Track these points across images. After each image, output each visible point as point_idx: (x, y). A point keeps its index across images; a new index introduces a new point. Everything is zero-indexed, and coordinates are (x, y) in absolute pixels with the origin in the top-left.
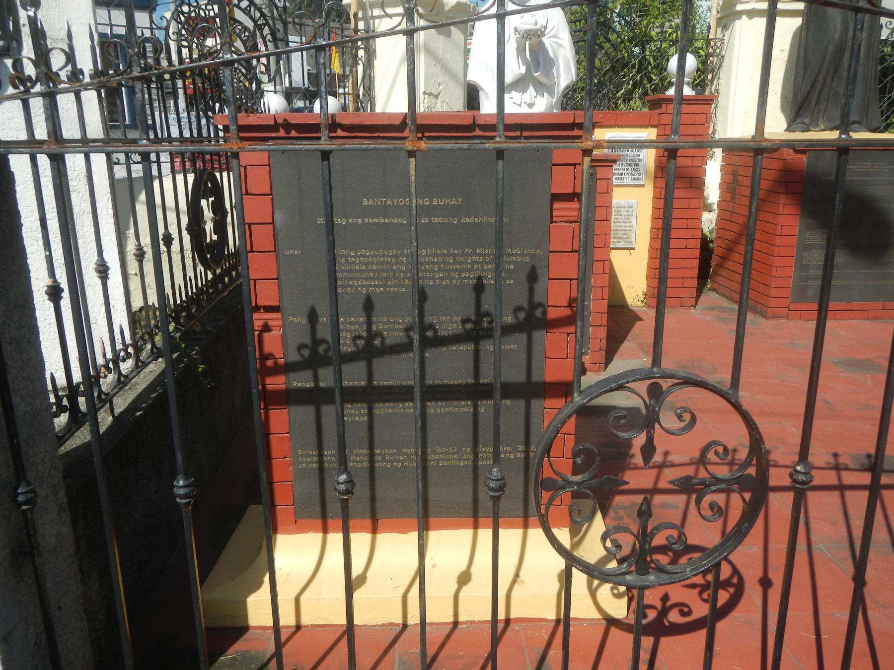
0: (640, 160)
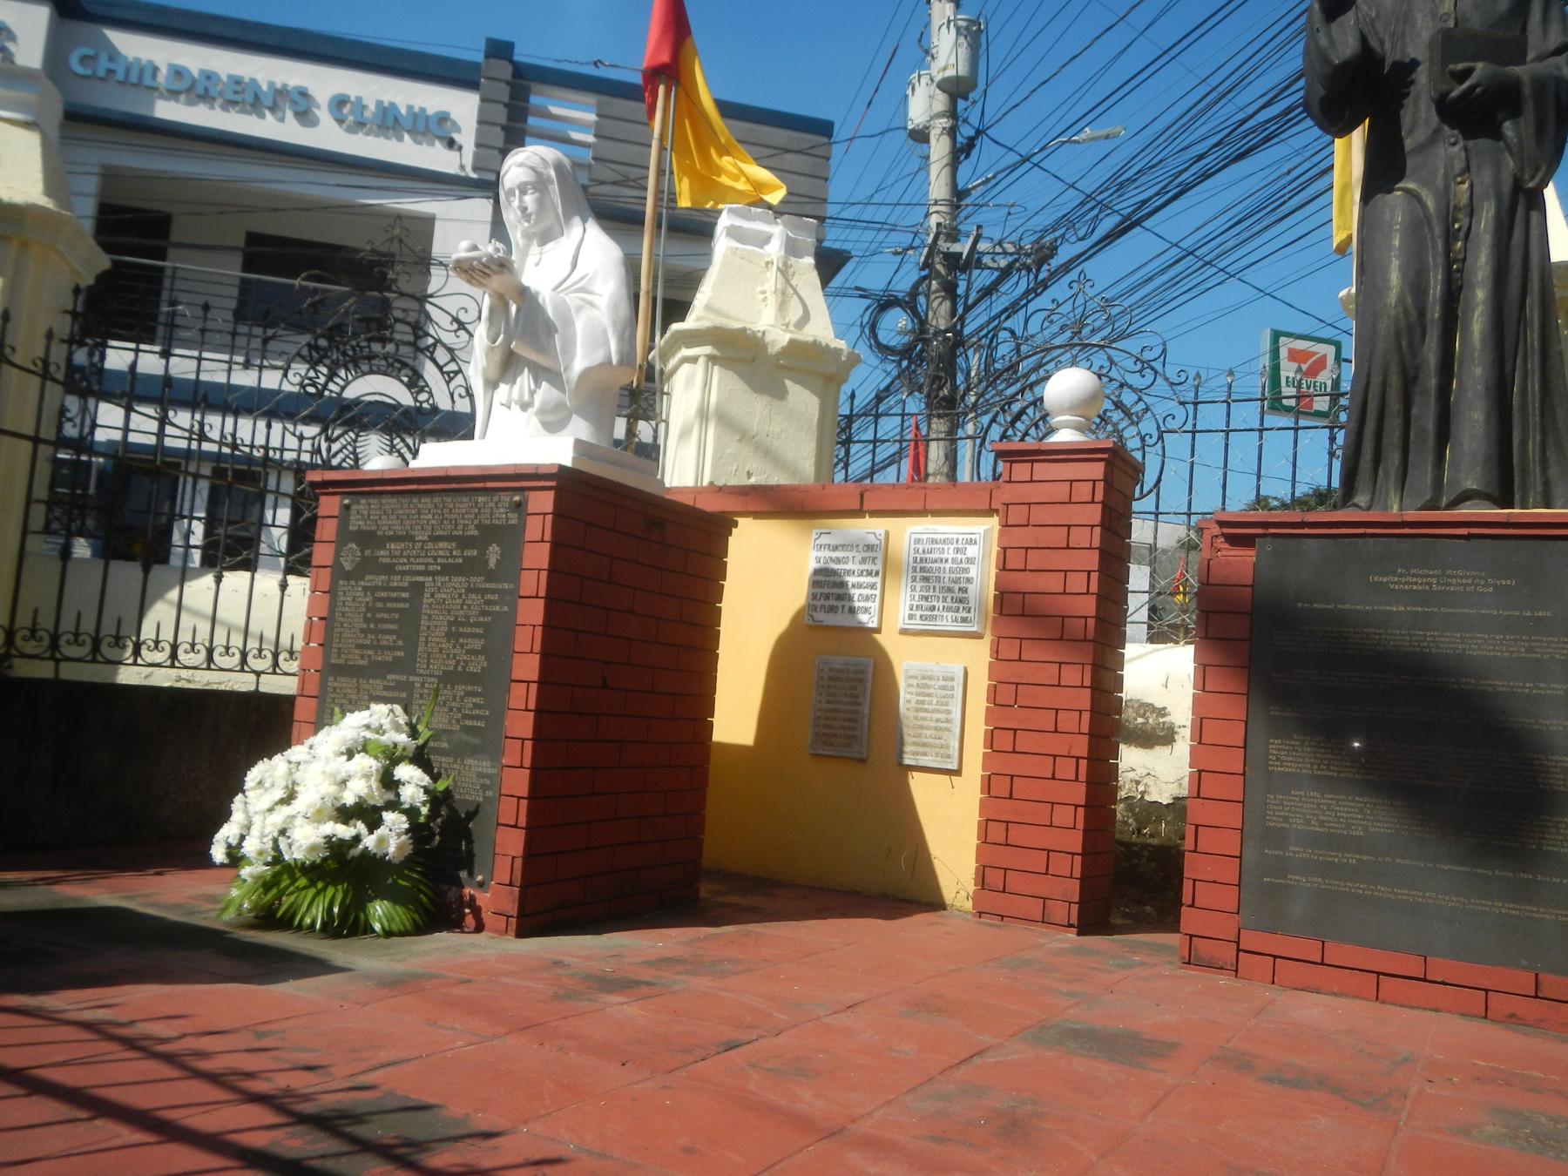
0: (969, 580)
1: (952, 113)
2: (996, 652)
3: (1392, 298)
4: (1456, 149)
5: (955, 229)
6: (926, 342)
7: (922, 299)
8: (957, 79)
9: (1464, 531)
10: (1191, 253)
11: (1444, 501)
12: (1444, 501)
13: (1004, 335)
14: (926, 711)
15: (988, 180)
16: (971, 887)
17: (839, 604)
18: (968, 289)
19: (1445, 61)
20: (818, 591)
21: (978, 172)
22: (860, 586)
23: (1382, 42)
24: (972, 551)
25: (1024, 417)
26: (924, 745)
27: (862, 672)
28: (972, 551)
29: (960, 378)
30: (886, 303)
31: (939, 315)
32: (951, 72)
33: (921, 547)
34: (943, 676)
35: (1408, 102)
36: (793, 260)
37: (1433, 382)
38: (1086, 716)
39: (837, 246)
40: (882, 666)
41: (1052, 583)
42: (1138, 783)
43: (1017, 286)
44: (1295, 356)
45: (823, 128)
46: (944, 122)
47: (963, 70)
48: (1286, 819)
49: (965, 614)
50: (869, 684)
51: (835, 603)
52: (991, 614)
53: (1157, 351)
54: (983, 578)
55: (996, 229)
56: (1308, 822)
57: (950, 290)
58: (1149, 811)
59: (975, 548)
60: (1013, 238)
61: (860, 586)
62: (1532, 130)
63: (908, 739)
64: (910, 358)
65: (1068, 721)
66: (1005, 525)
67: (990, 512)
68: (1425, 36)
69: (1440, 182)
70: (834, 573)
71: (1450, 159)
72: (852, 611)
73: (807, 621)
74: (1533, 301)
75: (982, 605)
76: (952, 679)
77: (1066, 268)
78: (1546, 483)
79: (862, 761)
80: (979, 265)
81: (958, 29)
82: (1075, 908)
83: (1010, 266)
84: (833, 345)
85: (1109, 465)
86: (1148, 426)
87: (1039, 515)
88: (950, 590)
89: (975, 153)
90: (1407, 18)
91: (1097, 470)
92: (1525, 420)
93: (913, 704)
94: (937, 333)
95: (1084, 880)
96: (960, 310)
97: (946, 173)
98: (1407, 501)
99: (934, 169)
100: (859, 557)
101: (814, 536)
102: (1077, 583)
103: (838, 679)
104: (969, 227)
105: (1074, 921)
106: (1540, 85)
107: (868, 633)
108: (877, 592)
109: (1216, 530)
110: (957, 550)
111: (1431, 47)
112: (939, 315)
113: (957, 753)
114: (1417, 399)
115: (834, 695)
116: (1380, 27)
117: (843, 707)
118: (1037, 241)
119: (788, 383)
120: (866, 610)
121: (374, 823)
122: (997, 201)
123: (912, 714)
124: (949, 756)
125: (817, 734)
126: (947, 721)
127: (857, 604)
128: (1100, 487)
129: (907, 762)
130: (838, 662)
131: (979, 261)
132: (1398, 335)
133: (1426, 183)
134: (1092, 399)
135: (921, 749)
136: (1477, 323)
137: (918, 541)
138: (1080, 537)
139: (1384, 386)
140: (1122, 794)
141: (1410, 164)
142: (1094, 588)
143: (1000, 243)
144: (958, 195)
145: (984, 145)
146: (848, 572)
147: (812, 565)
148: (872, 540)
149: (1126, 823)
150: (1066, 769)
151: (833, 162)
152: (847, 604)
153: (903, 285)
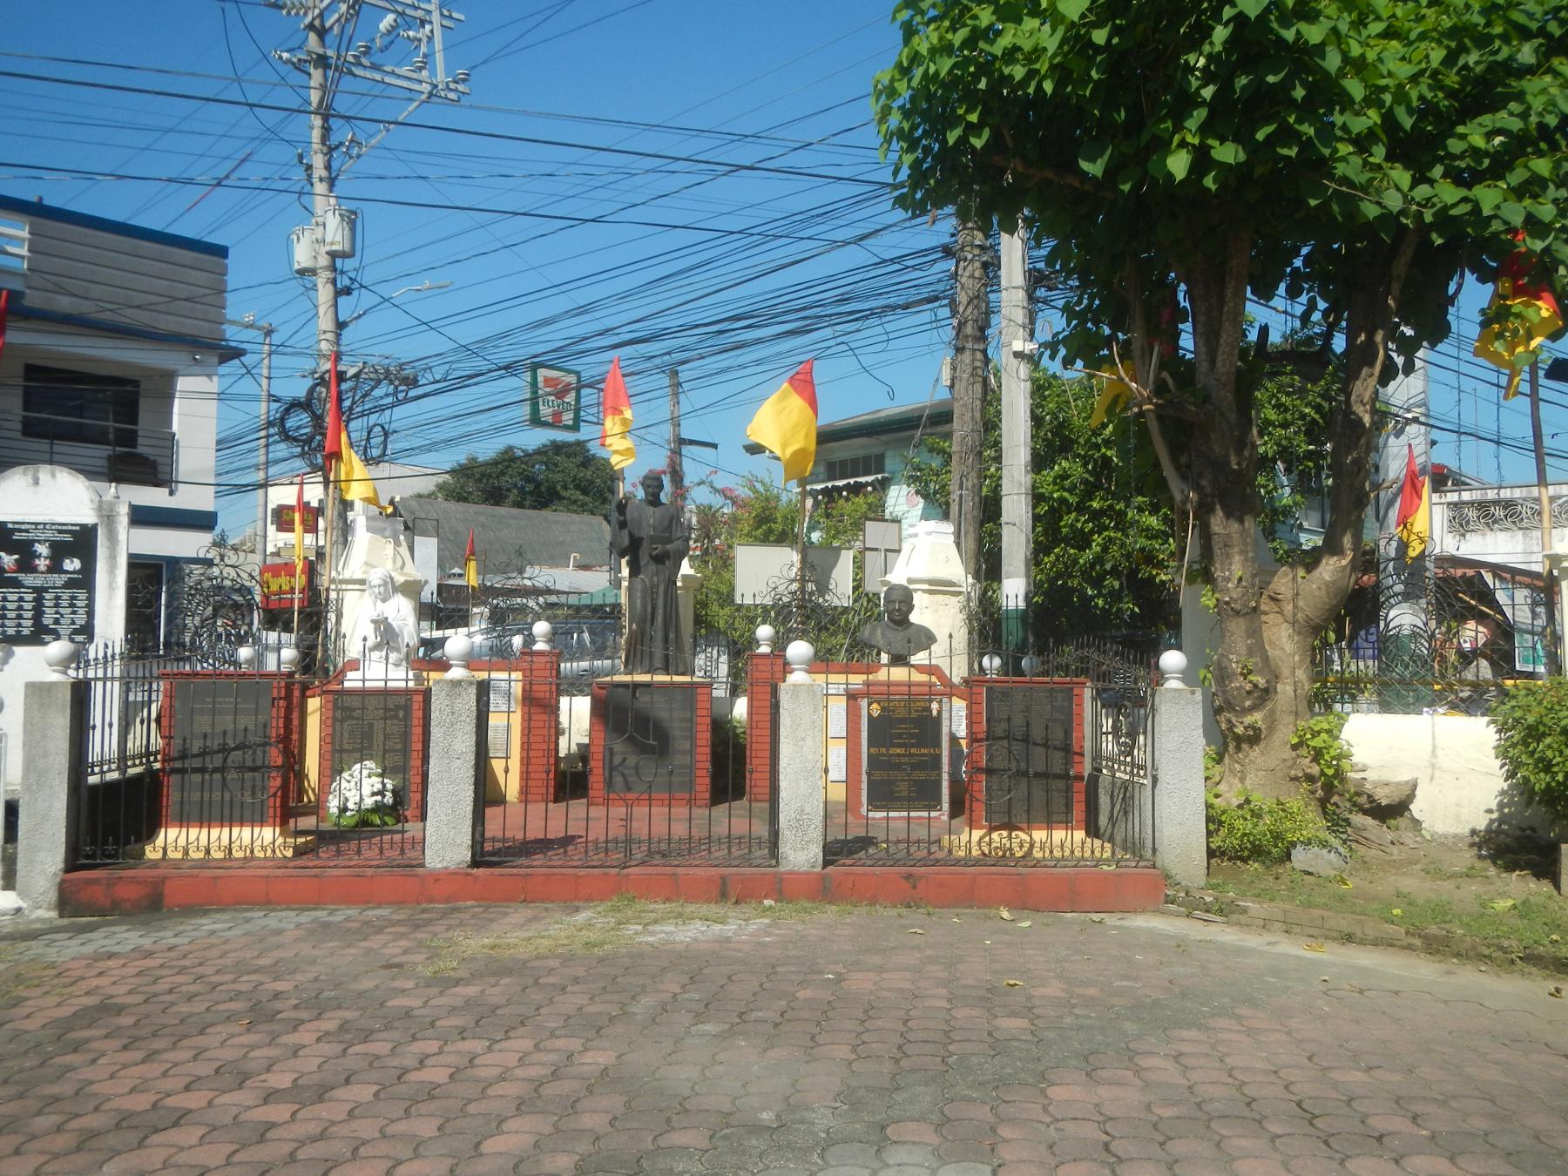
45: (221, 252)
121: (384, 796)
144: (341, 326)
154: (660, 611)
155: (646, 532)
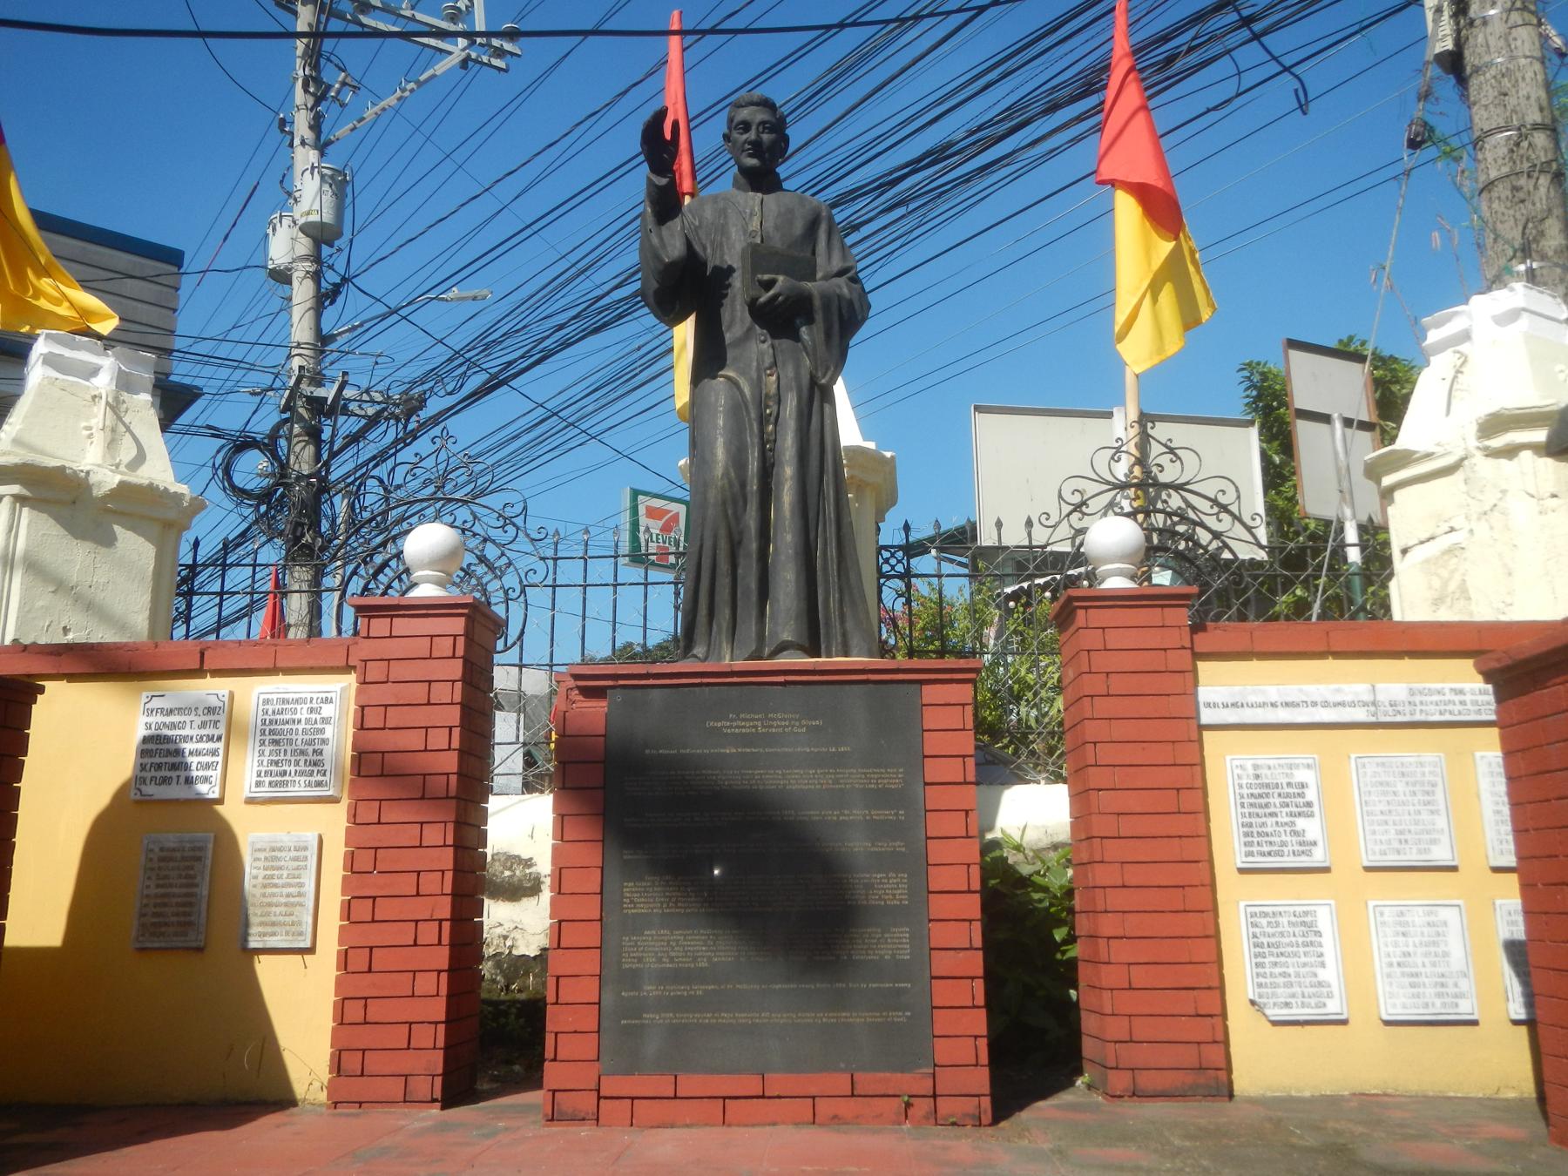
0: (324, 742)
1: (317, 258)
2: (353, 816)
3: (719, 470)
4: (765, 346)
5: (319, 373)
6: (287, 486)
7: (283, 442)
8: (321, 225)
9: (781, 679)
10: (556, 414)
11: (767, 651)
12: (767, 651)
13: (371, 483)
14: (276, 886)
15: (354, 328)
16: (324, 1074)
17: (174, 774)
18: (333, 435)
19: (754, 272)
20: (148, 760)
21: (344, 319)
22: (198, 753)
23: (705, 249)
24: (328, 710)
25: (387, 570)
26: (273, 924)
27: (200, 849)
28: (328, 710)
29: (325, 525)
30: (243, 444)
31: (303, 460)
32: (314, 218)
33: (270, 708)
34: (292, 846)
35: (726, 302)
36: (125, 396)
37: (754, 546)
38: (449, 876)
39: (187, 381)
40: (225, 839)
41: (413, 740)
42: (505, 938)
43: (386, 434)
44: (652, 513)
45: (174, 257)
46: (309, 266)
47: (328, 217)
48: (640, 960)
49: (320, 778)
50: (208, 862)
51: (168, 774)
52: (348, 777)
53: (518, 508)
54: (339, 738)
55: (364, 375)
56: (660, 960)
57: (314, 435)
58: (517, 966)
59: (331, 706)
60: (381, 387)
61: (198, 753)
62: (822, 336)
63: (253, 920)
64: (269, 504)
65: (430, 883)
66: (363, 682)
67: (347, 669)
68: (739, 247)
69: (754, 375)
70: (167, 739)
71: (761, 354)
72: (189, 781)
73: (133, 795)
74: (828, 478)
75: (338, 765)
76: (306, 849)
77: (435, 420)
78: (844, 635)
79: (200, 950)
80: (345, 411)
81: (322, 176)
82: (438, 1080)
83: (378, 414)
84: (172, 489)
85: (470, 620)
86: (510, 580)
87: (398, 671)
88: (303, 753)
89: (340, 299)
90: (723, 230)
91: (457, 625)
92: (827, 581)
93: (260, 879)
94: (300, 477)
95: (448, 1049)
96: (325, 456)
97: (309, 318)
98: (736, 652)
99: (297, 312)
100: (198, 721)
101: (144, 700)
102: (439, 739)
103: (171, 859)
104: (334, 372)
105: (438, 1094)
106: (827, 300)
107: (207, 806)
108: (220, 759)
109: (572, 683)
110: (312, 710)
111: (743, 258)
112: (303, 460)
113: (310, 930)
114: (742, 561)
115: (166, 877)
116: (702, 234)
117: (175, 890)
118: (406, 392)
119: (116, 528)
120: (206, 780)
122: (363, 349)
123: (258, 892)
124: (301, 934)
125: (143, 925)
126: (300, 895)
127: (195, 774)
128: (461, 641)
129: (253, 945)
130: (170, 840)
131: (345, 406)
132: (724, 503)
133: (743, 373)
134: (452, 554)
135: (269, 929)
136: (787, 495)
137: (267, 702)
138: (442, 693)
139: (715, 548)
140: (488, 951)
141: (730, 354)
142: (456, 744)
143: (367, 391)
144: (323, 340)
145: (350, 295)
146: (186, 739)
147: (141, 732)
148: (214, 702)
149: (494, 981)
150: (428, 933)
151: (184, 293)
152: (183, 774)
153: (263, 425)
154: (788, 471)
155: (732, 254)
